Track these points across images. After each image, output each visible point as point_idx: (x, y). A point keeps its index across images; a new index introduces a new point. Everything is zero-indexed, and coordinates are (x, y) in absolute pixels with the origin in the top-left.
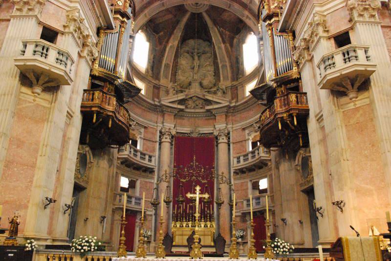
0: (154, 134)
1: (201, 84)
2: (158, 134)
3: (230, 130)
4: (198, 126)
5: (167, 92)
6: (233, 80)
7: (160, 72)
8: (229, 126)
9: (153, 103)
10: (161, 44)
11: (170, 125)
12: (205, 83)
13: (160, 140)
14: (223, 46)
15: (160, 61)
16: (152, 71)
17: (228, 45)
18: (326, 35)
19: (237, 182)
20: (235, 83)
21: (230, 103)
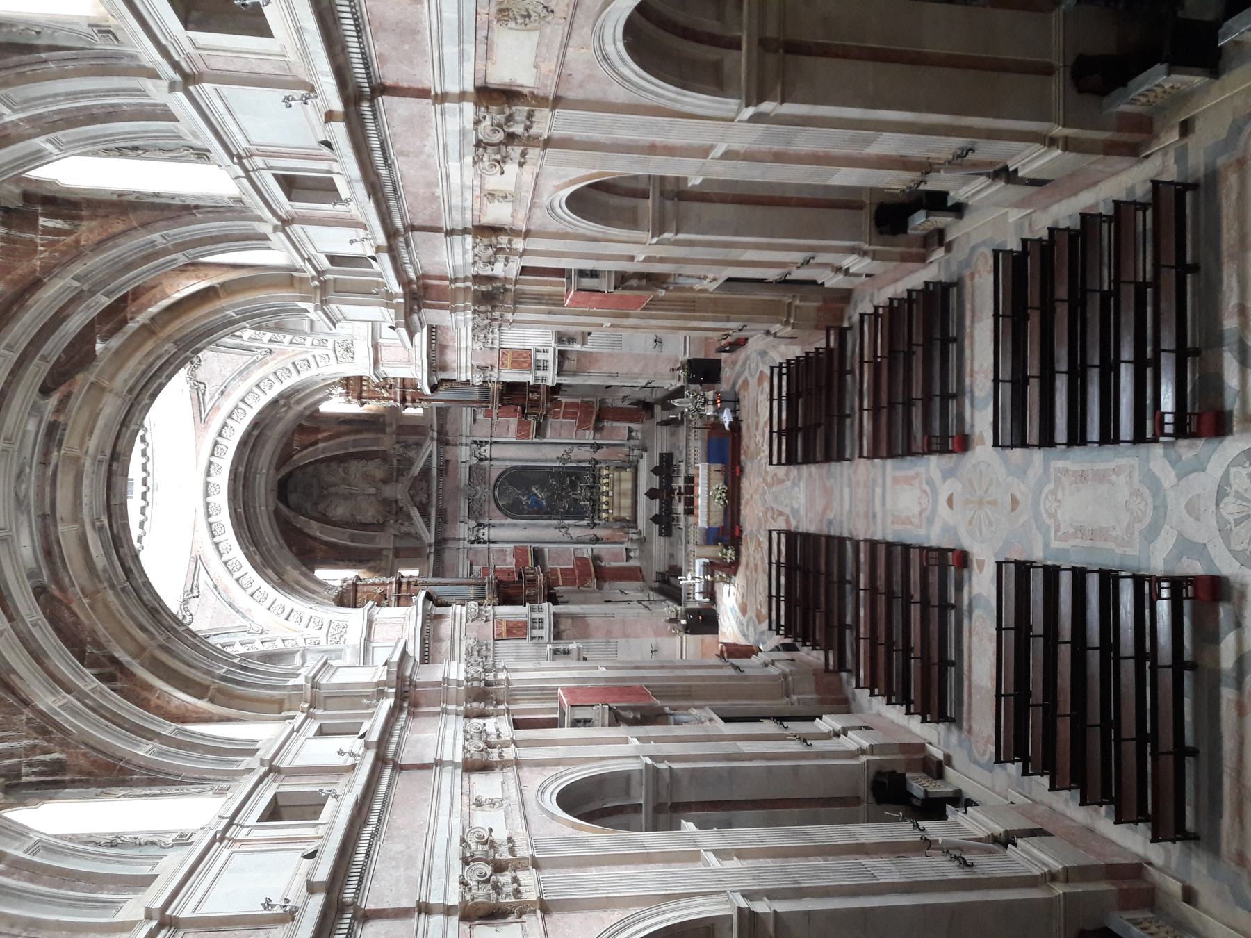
0: (477, 552)
1: (385, 482)
2: (476, 545)
3: (469, 440)
4: (457, 487)
5: (409, 534)
6: (383, 431)
7: (364, 549)
8: (464, 440)
9: (432, 557)
10: (312, 550)
11: (464, 530)
12: (379, 474)
13: (485, 542)
14: (321, 445)
15: (347, 548)
16: (368, 561)
17: (320, 436)
18: (496, 370)
19: (548, 435)
20: (388, 430)
21: (432, 439)
